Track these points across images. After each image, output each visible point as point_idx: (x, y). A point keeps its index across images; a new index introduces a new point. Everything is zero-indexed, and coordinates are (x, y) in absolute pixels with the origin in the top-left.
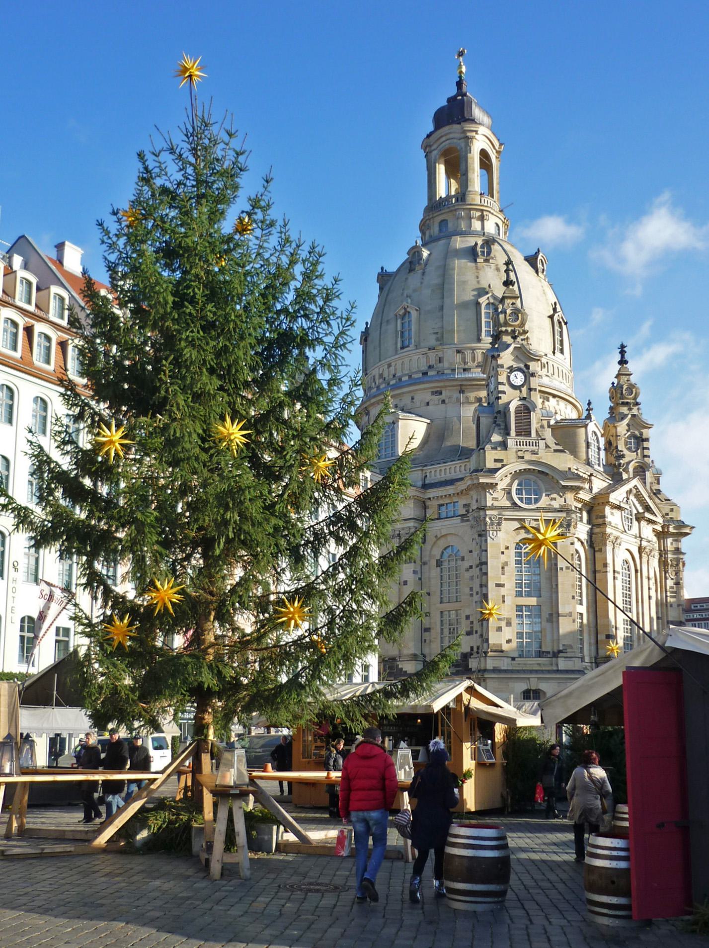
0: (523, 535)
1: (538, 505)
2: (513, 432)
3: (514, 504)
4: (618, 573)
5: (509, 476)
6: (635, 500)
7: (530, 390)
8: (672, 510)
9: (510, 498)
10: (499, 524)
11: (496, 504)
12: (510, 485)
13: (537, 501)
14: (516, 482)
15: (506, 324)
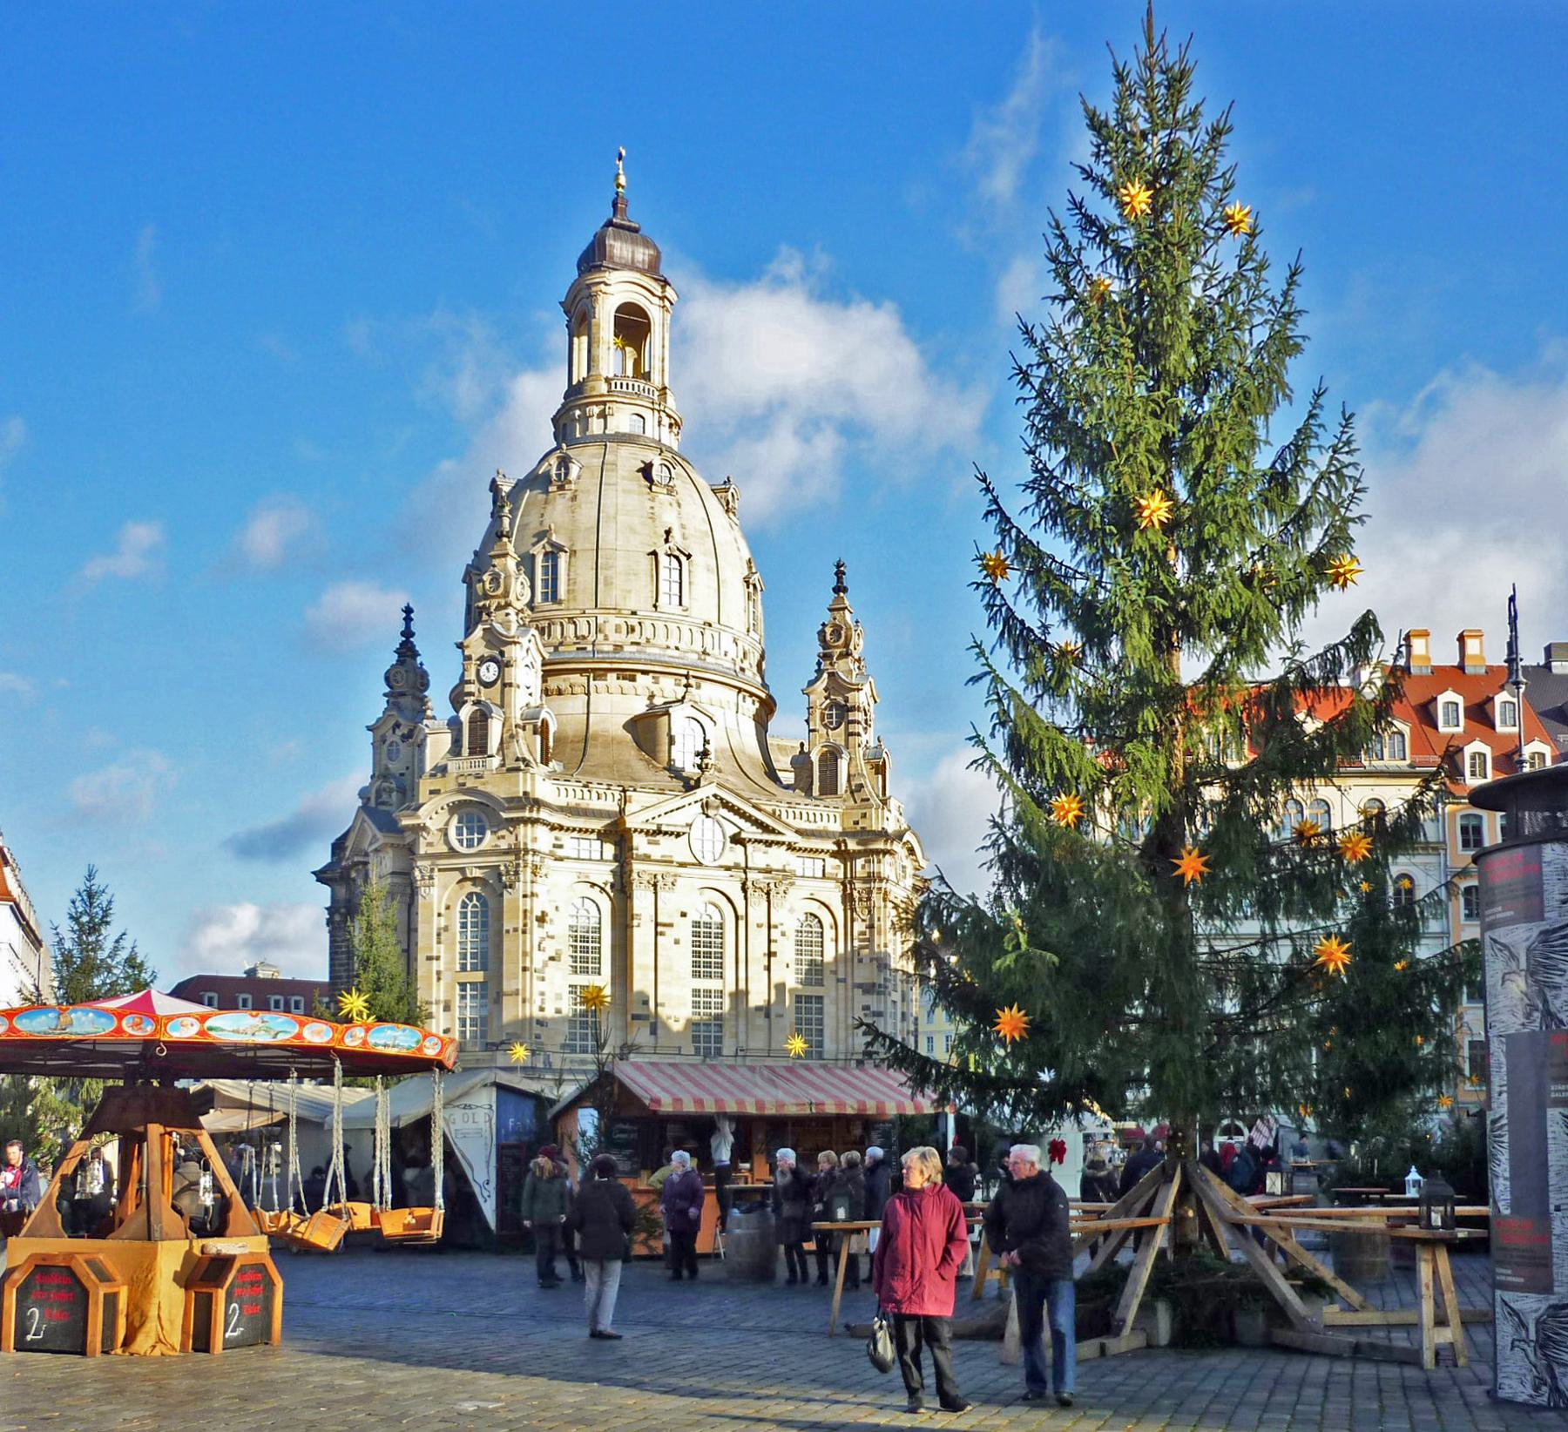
0: (469, 887)
1: (485, 846)
2: (465, 751)
3: (451, 849)
4: (671, 925)
5: (445, 815)
6: (724, 812)
7: (504, 685)
8: (864, 816)
9: (447, 842)
10: (431, 878)
11: (431, 850)
12: (447, 824)
13: (480, 840)
14: (455, 819)
15: (486, 596)
